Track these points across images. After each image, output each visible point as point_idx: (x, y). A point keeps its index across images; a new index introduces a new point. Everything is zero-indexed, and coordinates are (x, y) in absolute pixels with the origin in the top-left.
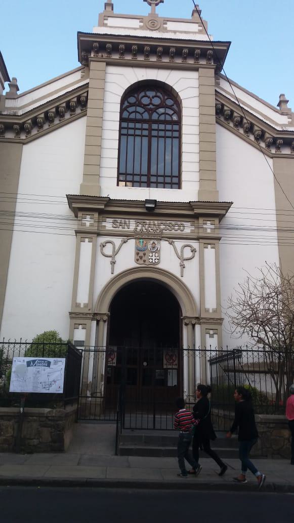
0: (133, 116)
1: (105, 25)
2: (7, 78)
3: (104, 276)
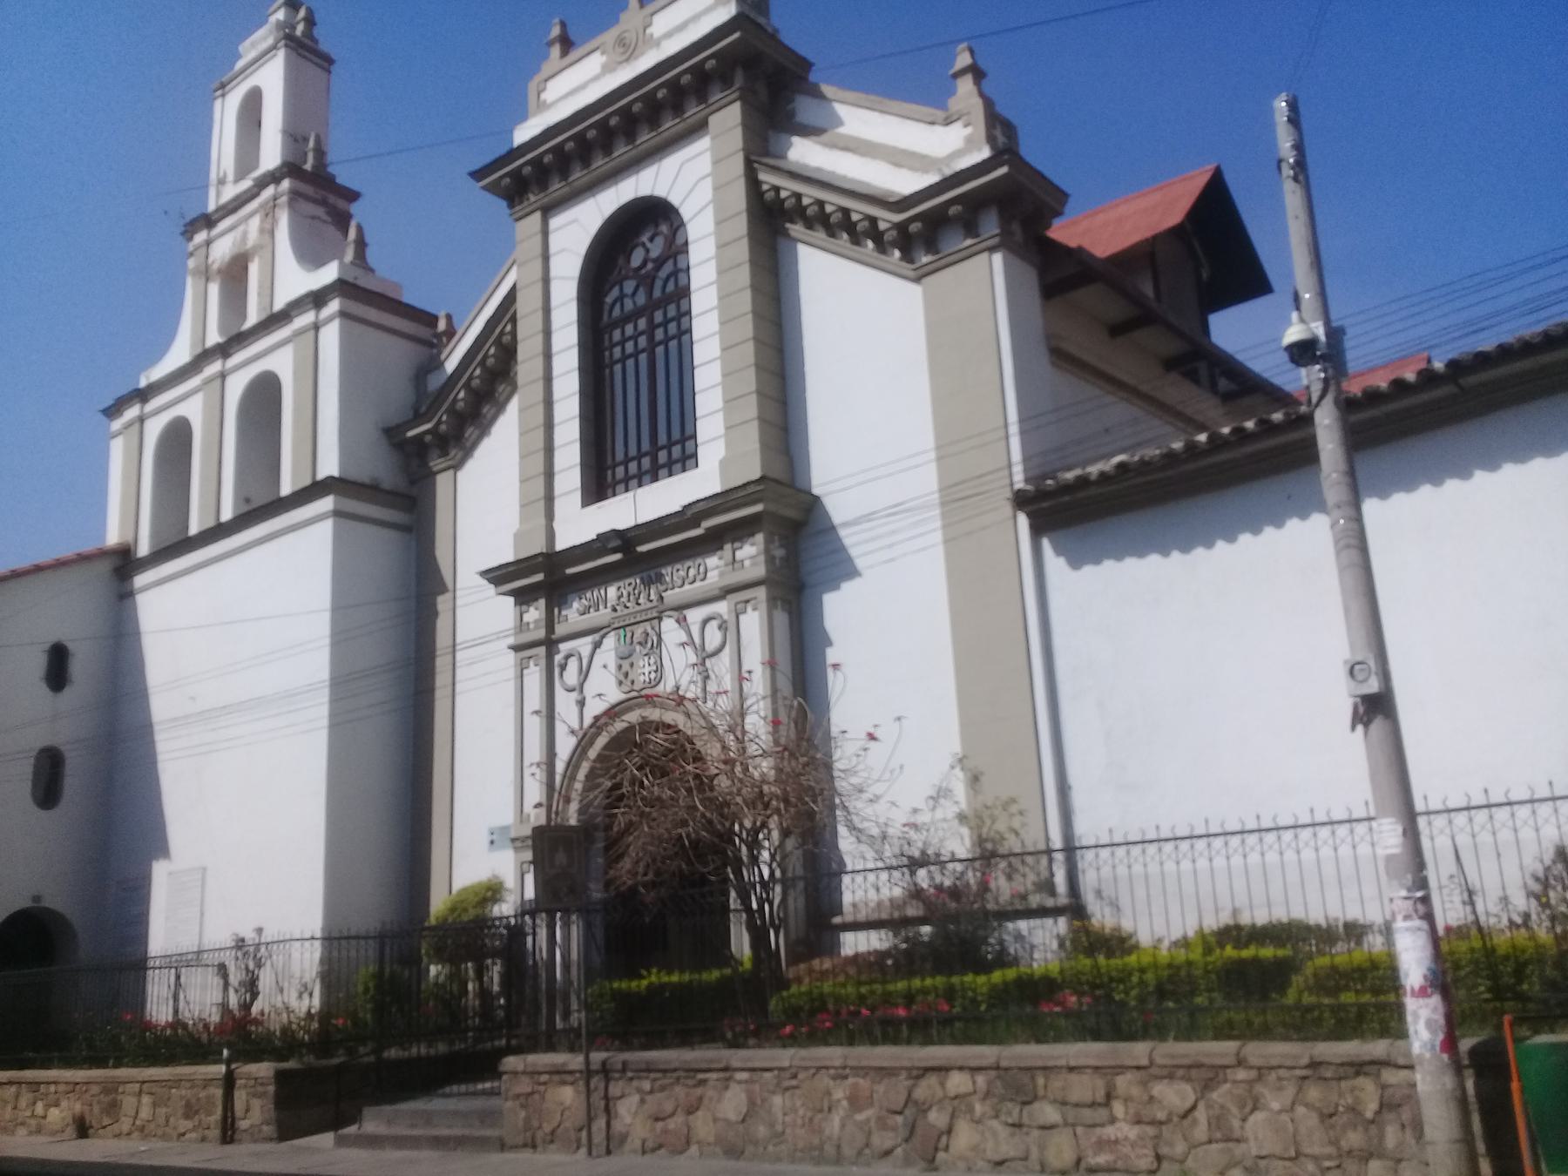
0: (617, 312)
1: (543, 107)
2: (430, 320)
3: (565, 746)
